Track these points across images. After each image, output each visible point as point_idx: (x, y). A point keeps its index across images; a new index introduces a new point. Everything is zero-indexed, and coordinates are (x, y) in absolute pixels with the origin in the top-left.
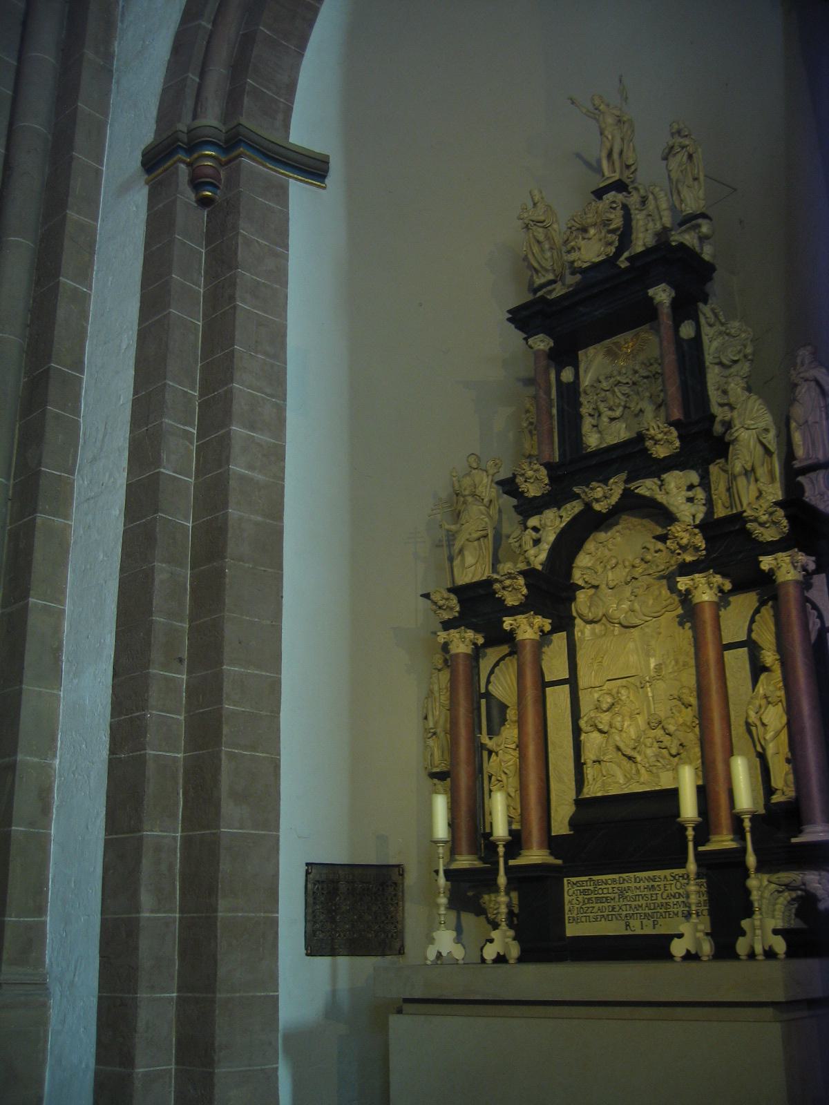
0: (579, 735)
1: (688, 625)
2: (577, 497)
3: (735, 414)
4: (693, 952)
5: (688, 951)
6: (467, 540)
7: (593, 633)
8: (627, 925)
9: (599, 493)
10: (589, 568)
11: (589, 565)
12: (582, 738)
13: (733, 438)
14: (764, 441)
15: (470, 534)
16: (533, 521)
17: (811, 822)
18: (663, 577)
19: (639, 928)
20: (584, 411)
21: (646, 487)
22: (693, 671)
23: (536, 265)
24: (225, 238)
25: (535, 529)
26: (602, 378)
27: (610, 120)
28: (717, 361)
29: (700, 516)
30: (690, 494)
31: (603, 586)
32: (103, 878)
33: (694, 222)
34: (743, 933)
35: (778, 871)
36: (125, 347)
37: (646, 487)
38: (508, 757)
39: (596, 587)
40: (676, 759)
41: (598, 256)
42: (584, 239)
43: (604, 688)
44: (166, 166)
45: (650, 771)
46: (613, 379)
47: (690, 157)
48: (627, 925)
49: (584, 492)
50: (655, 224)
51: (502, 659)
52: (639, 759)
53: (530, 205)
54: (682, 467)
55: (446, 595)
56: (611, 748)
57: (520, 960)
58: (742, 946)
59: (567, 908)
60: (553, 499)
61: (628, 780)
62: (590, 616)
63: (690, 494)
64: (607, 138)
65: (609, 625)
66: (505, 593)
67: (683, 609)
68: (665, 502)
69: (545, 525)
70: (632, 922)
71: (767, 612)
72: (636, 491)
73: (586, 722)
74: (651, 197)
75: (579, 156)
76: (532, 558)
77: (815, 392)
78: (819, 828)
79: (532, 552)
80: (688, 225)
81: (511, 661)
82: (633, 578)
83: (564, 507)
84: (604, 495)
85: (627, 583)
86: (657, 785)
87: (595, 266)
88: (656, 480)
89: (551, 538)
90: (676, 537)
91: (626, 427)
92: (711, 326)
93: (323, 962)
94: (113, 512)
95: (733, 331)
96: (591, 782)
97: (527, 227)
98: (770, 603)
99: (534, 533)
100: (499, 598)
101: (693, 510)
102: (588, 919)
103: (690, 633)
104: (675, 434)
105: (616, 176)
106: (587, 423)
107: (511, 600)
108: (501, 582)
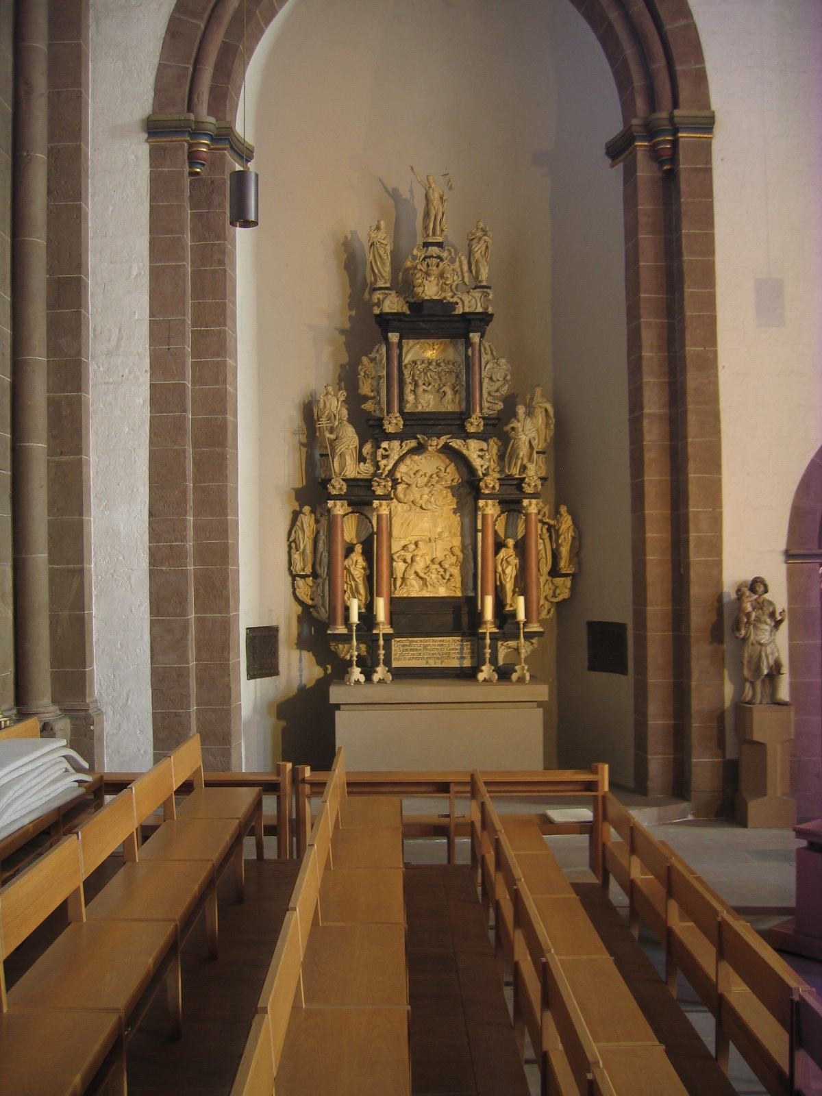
0: (392, 563)
1: (458, 514)
2: (418, 439)
3: (519, 424)
4: (487, 678)
5: (485, 679)
6: (347, 449)
7: (403, 508)
8: (427, 663)
9: (434, 443)
10: (406, 473)
11: (406, 471)
12: (394, 564)
13: (516, 437)
14: (533, 444)
15: (349, 446)
16: (385, 445)
17: (531, 622)
18: (449, 487)
19: (432, 664)
20: (408, 381)
21: (456, 444)
22: (460, 538)
23: (376, 271)
24: (211, 210)
25: (385, 449)
26: (418, 363)
27: (436, 196)
28: (489, 376)
29: (485, 467)
30: (480, 453)
31: (414, 486)
32: (151, 643)
33: (485, 290)
34: (516, 671)
35: (507, 641)
36: (135, 274)
37: (456, 444)
38: (357, 572)
39: (407, 484)
40: (445, 581)
41: (435, 295)
42: (427, 280)
43: (407, 539)
44: (174, 139)
45: (434, 587)
46: (423, 365)
47: (487, 247)
48: (427, 663)
49: (424, 439)
50: (458, 278)
51: (347, 514)
52: (428, 579)
53: (373, 228)
54: (479, 439)
55: (342, 482)
56: (412, 571)
57: (391, 682)
58: (514, 677)
59: (393, 653)
60: (401, 437)
61: (421, 590)
62: (406, 501)
63: (480, 453)
64: (434, 207)
65: (413, 506)
66: (378, 488)
67: (457, 504)
68: (467, 455)
69: (393, 449)
70: (430, 661)
71: (503, 516)
72: (451, 444)
73: (398, 557)
74: (457, 259)
75: (381, 181)
76: (382, 467)
77: (544, 414)
78: (535, 625)
79: (383, 463)
80: (482, 290)
81: (351, 516)
82: (432, 485)
83: (405, 442)
84: (435, 443)
85: (426, 485)
86: (436, 593)
87: (432, 301)
88: (463, 441)
89: (396, 457)
90: (485, 482)
91: (434, 399)
92: (486, 354)
93: (253, 681)
94: (137, 400)
95: (501, 364)
96: (398, 588)
97: (372, 244)
98: (506, 513)
99: (384, 451)
100: (373, 490)
101: (482, 463)
102: (405, 659)
103: (459, 519)
104: (482, 423)
105: (440, 239)
106: (409, 388)
107: (379, 491)
108: (378, 482)
